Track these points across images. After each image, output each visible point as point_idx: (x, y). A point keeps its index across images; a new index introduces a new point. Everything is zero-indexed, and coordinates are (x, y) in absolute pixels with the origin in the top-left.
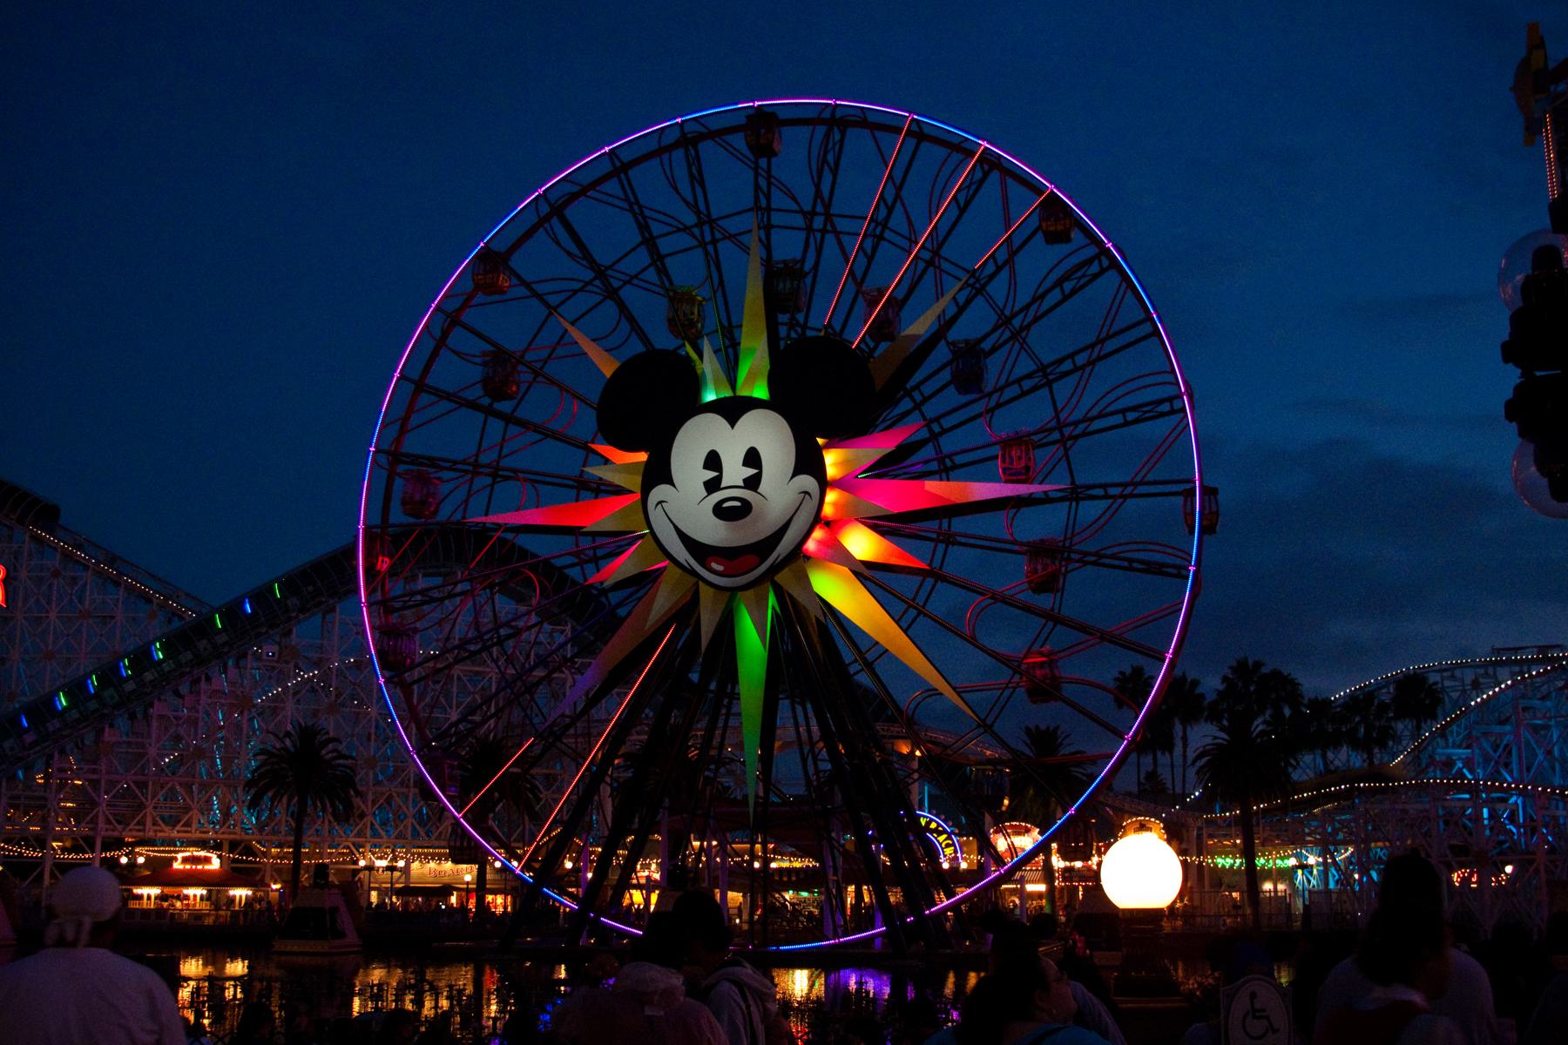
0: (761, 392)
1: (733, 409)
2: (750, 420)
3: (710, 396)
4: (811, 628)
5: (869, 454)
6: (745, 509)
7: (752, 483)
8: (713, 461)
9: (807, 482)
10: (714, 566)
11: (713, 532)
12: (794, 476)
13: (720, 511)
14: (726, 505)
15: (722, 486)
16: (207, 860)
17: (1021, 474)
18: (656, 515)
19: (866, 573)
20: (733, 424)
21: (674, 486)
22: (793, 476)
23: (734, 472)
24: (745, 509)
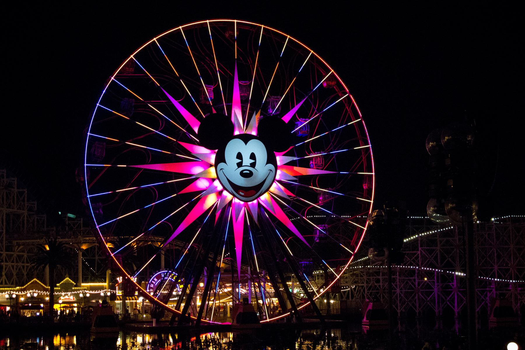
1: (246, 138)
3: (237, 133)
5: (289, 159)
7: (253, 165)
8: (239, 156)
9: (271, 166)
10: (241, 193)
11: (241, 181)
13: (242, 174)
14: (244, 172)
15: (243, 165)
17: (320, 166)
18: (220, 174)
20: (246, 144)
21: (226, 163)
22: (266, 164)
23: (247, 161)
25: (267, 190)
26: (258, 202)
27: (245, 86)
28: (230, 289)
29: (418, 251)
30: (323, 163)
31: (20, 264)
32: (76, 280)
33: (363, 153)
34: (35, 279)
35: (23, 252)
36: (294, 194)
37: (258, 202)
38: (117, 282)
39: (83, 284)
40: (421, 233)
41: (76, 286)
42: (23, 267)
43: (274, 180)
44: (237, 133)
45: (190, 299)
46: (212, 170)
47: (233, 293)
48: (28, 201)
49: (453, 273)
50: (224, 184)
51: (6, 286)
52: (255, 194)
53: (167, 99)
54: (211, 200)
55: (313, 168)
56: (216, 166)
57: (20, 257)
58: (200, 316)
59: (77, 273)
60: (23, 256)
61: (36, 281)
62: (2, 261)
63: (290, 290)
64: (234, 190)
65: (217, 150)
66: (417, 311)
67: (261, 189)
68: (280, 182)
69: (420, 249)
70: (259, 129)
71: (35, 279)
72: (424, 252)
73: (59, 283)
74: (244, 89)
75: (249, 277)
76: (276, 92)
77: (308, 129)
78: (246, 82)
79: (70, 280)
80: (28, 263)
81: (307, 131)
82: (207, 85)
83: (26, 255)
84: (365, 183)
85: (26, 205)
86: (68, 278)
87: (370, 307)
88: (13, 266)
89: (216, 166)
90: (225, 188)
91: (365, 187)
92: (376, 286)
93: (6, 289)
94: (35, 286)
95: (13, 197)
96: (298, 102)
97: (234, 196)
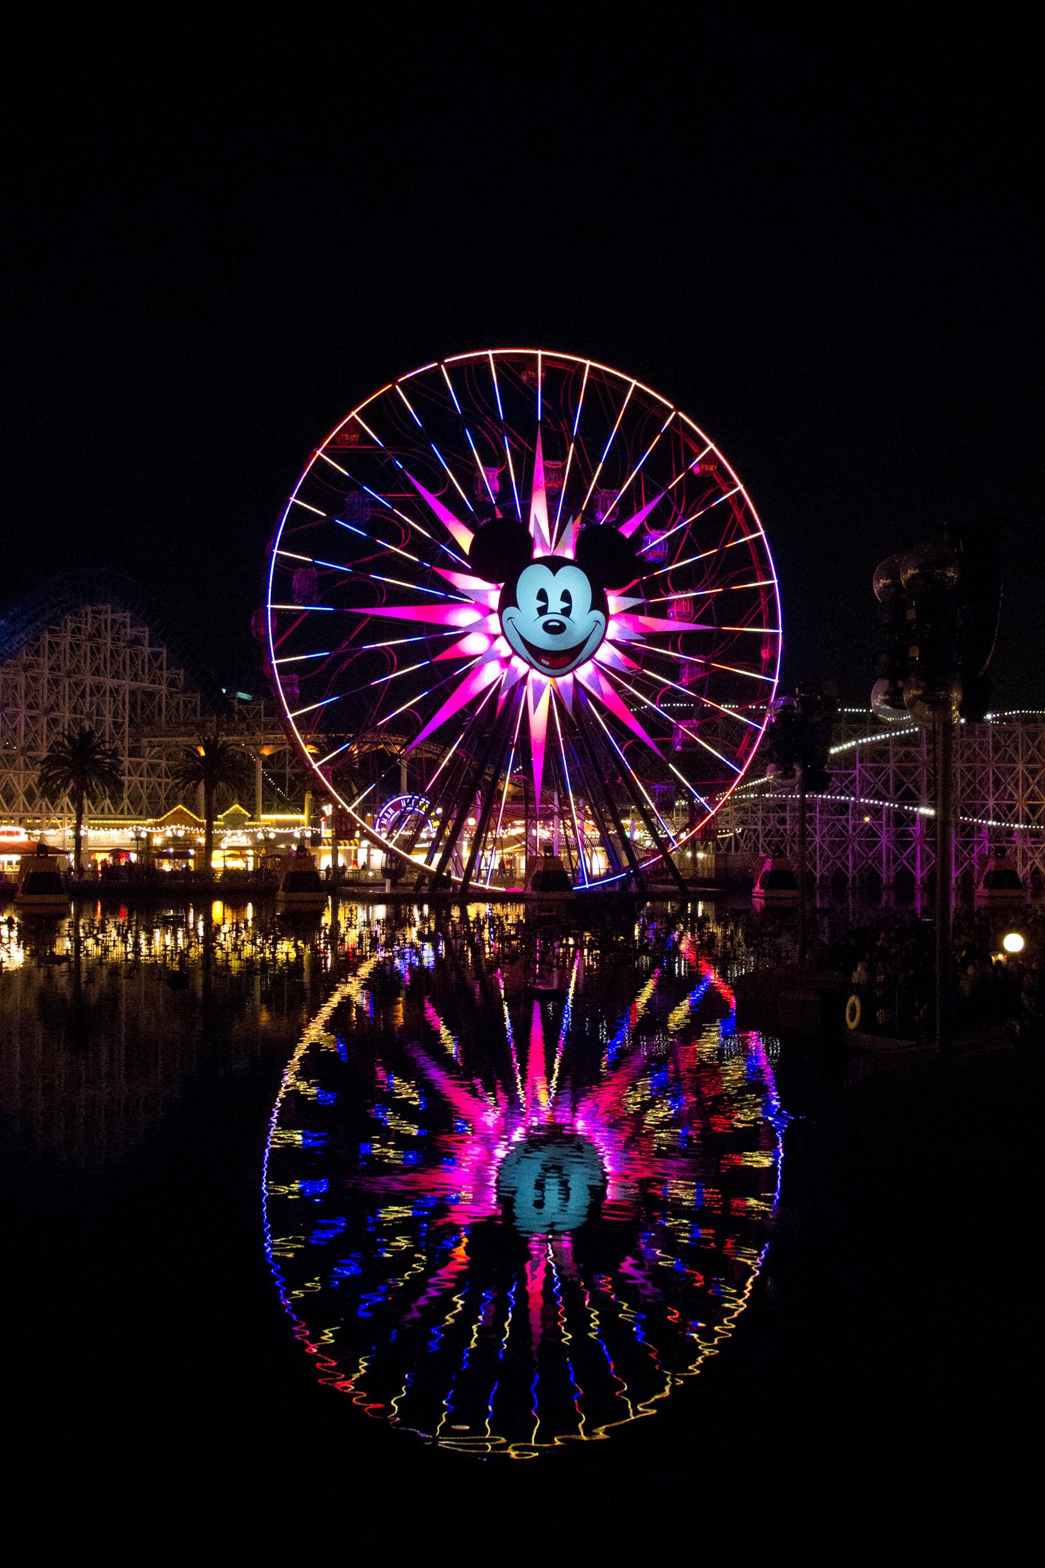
0: (569, 554)
1: (555, 564)
2: (565, 571)
3: (538, 553)
5: (631, 602)
6: (560, 629)
7: (566, 612)
8: (542, 595)
9: (598, 615)
10: (543, 661)
11: (544, 641)
12: (591, 610)
13: (546, 627)
14: (550, 624)
16: (18, 833)
17: (686, 616)
18: (507, 625)
20: (554, 573)
21: (518, 607)
22: (591, 610)
23: (556, 604)
24: (560, 629)
25: (591, 656)
26: (574, 676)
27: (553, 470)
28: (521, 830)
29: (855, 768)
30: (692, 611)
31: (154, 779)
32: (251, 808)
33: (762, 594)
34: (180, 806)
35: (160, 757)
36: (638, 664)
37: (575, 680)
38: (323, 814)
39: (263, 817)
40: (862, 738)
41: (251, 819)
42: (160, 784)
43: (603, 639)
44: (538, 553)
45: (450, 847)
46: (493, 620)
47: (526, 837)
48: (168, 669)
49: (916, 809)
50: (514, 646)
51: (128, 817)
52: (568, 665)
53: (414, 490)
54: (491, 674)
55: (673, 619)
56: (500, 612)
57: (153, 767)
58: (468, 876)
59: (253, 796)
60: (159, 765)
61: (182, 811)
62: (123, 774)
63: (628, 834)
64: (533, 657)
65: (502, 585)
66: (850, 876)
67: (576, 657)
68: (613, 642)
69: (858, 766)
70: (578, 549)
71: (180, 806)
72: (866, 771)
73: (222, 814)
74: (554, 475)
75: (556, 810)
76: (611, 480)
77: (665, 549)
78: (557, 463)
79: (240, 808)
80: (168, 777)
81: (665, 553)
82: (487, 468)
83: (164, 763)
84: (766, 648)
85: (165, 677)
86: (237, 806)
87: (768, 865)
88: (142, 783)
89: (500, 612)
90: (515, 652)
91: (765, 654)
92: (779, 830)
93: (129, 822)
94: (180, 819)
95: (143, 661)
96: (649, 500)
97: (532, 666)
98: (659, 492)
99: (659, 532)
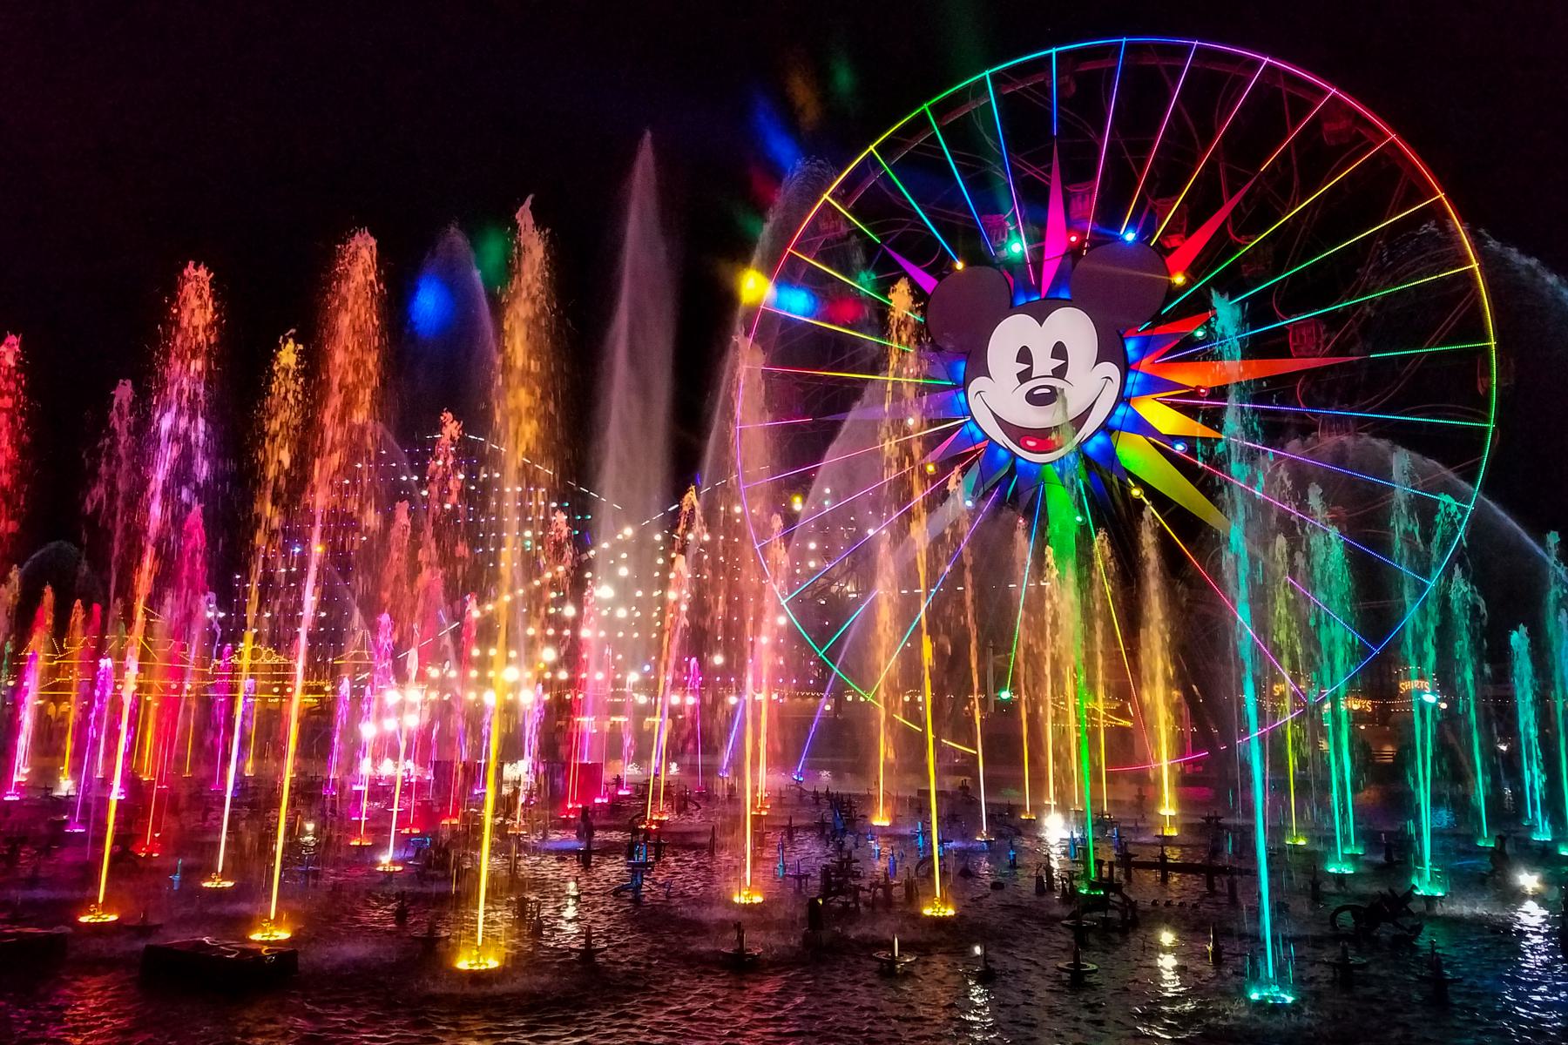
4: (1114, 492)
7: (1060, 373)
8: (1024, 355)
13: (1033, 399)
14: (1035, 393)
19: (1163, 444)
23: (1044, 364)
76: (1166, 185)
98: (1246, 179)
99: (1251, 237)
